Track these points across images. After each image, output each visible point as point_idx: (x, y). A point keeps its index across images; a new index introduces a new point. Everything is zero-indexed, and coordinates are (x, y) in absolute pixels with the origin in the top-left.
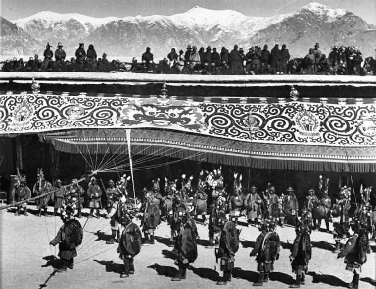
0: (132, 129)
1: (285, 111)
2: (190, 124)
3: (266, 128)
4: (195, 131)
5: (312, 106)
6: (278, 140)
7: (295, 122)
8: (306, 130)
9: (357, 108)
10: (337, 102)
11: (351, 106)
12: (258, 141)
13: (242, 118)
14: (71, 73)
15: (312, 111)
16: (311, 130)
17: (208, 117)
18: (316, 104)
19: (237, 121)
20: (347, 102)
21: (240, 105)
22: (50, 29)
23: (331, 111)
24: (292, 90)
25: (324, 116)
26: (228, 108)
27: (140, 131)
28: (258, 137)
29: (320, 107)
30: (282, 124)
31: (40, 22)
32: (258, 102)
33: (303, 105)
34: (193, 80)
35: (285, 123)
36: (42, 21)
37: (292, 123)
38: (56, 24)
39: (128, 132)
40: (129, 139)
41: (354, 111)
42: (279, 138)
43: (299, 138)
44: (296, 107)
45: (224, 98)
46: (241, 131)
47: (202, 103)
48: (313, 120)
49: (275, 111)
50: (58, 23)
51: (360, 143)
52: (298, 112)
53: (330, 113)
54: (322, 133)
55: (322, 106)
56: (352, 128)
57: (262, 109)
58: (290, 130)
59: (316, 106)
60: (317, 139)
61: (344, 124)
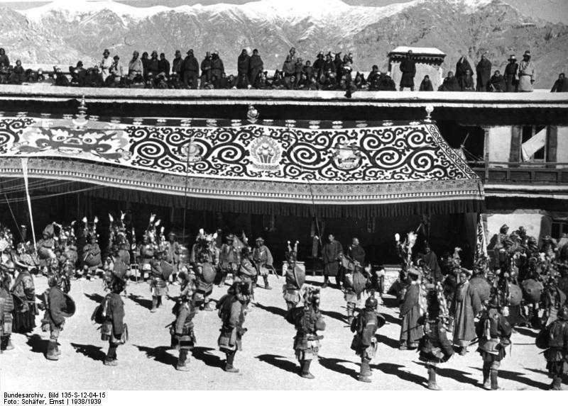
0: (30, 158)
1: (239, 137)
2: (109, 152)
3: (210, 159)
4: (112, 161)
5: (275, 130)
6: (223, 175)
7: (250, 151)
8: (262, 162)
9: (334, 134)
10: (307, 126)
11: (325, 130)
12: (196, 174)
13: (180, 146)
15: (274, 138)
16: (269, 162)
17: (136, 144)
18: (280, 128)
19: (173, 150)
20: (321, 126)
21: (181, 128)
22: (75, 23)
23: (299, 137)
24: (250, 109)
25: (289, 144)
26: (164, 132)
27: (40, 160)
28: (197, 170)
29: (285, 132)
31: (61, 13)
32: (204, 124)
33: (263, 129)
34: (127, 95)
35: (236, 153)
36: (64, 13)
37: (245, 153)
38: (82, 17)
39: (24, 162)
41: (329, 137)
42: (224, 172)
43: (251, 172)
44: (253, 132)
45: (161, 120)
46: (176, 162)
47: (130, 126)
48: (274, 150)
49: (225, 137)
50: (86, 15)
51: (330, 179)
52: (256, 139)
53: (297, 140)
54: (284, 165)
55: (287, 131)
56: (324, 160)
57: (209, 134)
58: (242, 162)
59: (281, 130)
60: (275, 174)
61: (314, 154)
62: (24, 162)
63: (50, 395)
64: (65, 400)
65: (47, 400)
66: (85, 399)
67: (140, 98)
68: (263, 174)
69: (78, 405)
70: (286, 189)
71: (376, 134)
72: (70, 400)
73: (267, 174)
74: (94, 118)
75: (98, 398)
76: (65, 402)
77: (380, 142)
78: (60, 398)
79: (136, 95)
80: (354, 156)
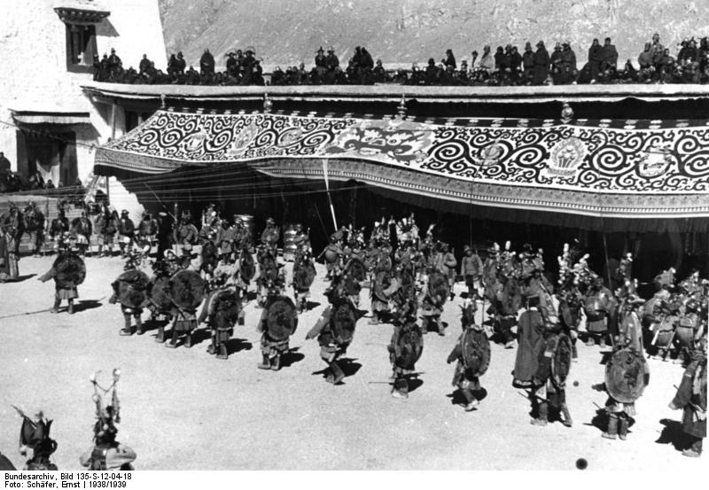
0: (330, 159)
1: (545, 138)
3: (506, 163)
4: (402, 164)
6: (512, 180)
7: (551, 154)
9: (649, 134)
11: (640, 131)
12: (484, 180)
13: (481, 148)
14: (611, 86)
15: (583, 140)
17: (439, 144)
19: (473, 152)
20: (638, 126)
21: (490, 128)
23: (609, 139)
24: (565, 108)
25: (597, 146)
26: (472, 133)
29: (597, 133)
30: (613, 158)
32: (515, 124)
33: (573, 129)
34: (461, 93)
37: (546, 155)
39: (325, 163)
40: (326, 173)
41: (642, 139)
42: (514, 178)
44: (562, 133)
46: (469, 164)
47: (441, 126)
52: (562, 140)
53: (607, 142)
54: (581, 170)
56: (629, 165)
57: (516, 135)
58: (538, 166)
59: (592, 131)
60: (567, 181)
61: (619, 158)
62: (325, 163)
63: (63, 476)
64: (82, 482)
65: (59, 483)
67: (475, 96)
68: (554, 180)
69: (97, 488)
70: (574, 198)
71: (695, 135)
73: (559, 180)
74: (411, 118)
75: (122, 480)
76: (82, 485)
77: (698, 144)
78: (75, 480)
79: (472, 93)
80: (663, 161)
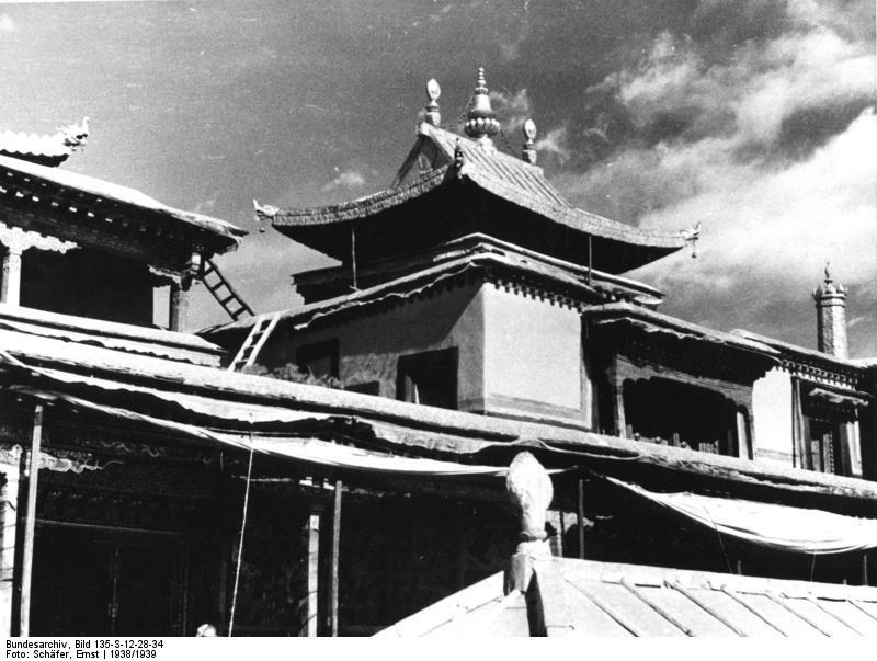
63: (77, 644)
64: (101, 651)
65: (73, 652)
66: (132, 650)
72: (108, 651)
75: (150, 648)
76: (101, 654)
78: (93, 649)
